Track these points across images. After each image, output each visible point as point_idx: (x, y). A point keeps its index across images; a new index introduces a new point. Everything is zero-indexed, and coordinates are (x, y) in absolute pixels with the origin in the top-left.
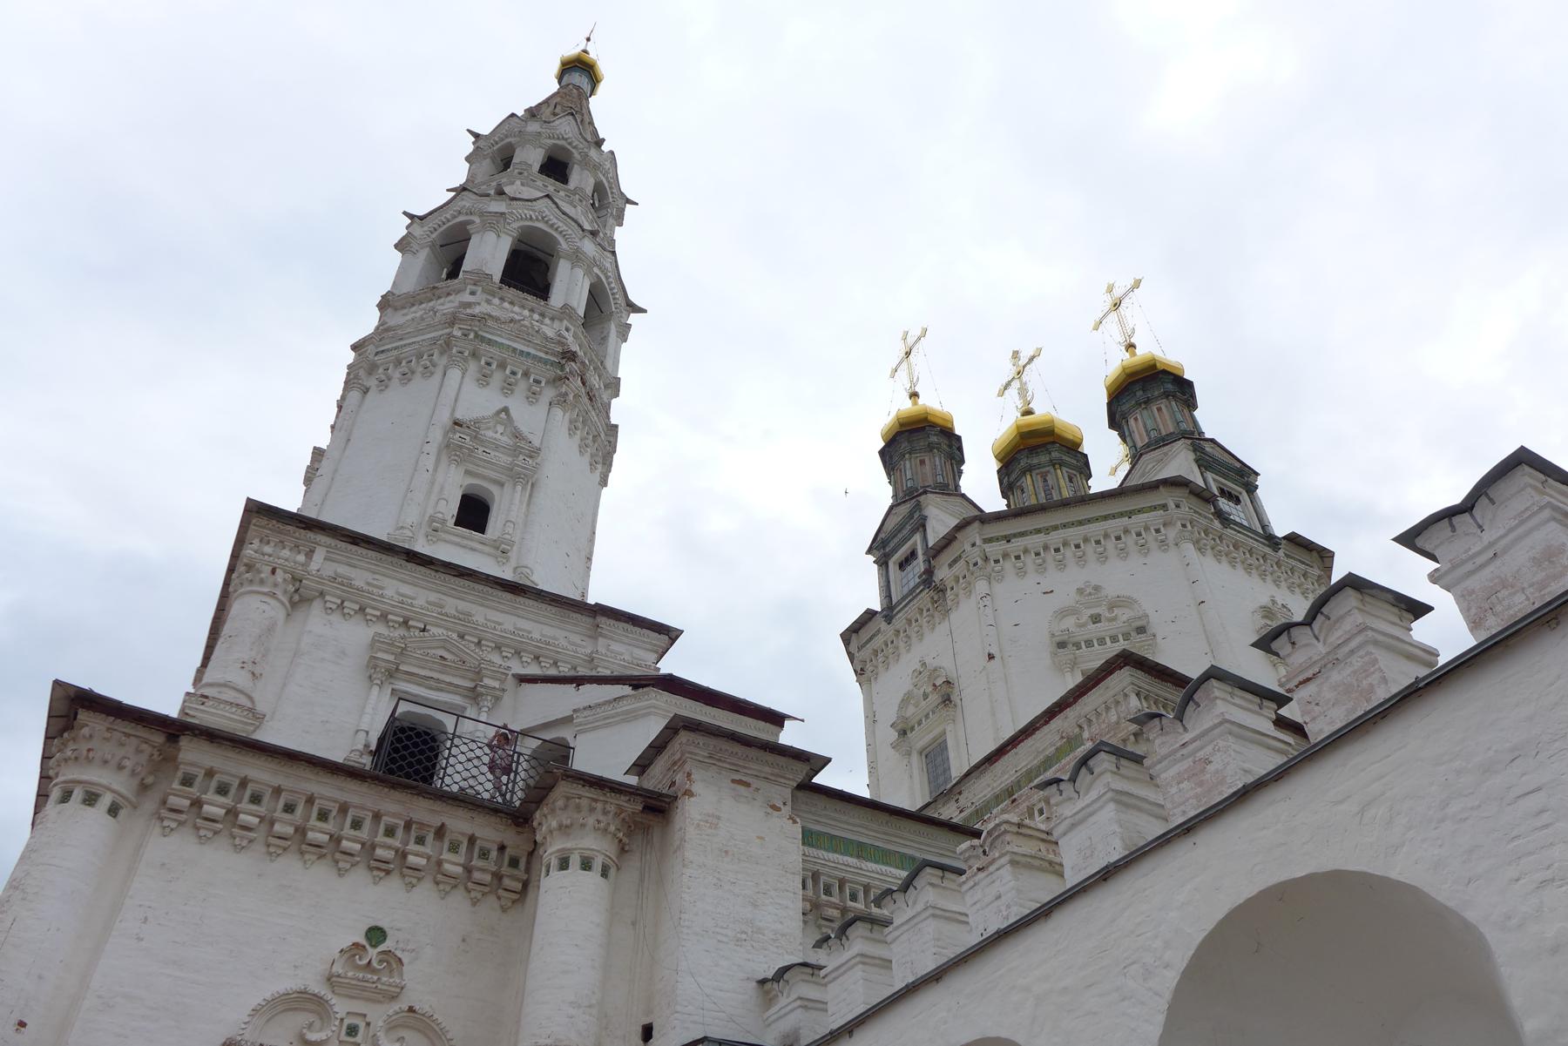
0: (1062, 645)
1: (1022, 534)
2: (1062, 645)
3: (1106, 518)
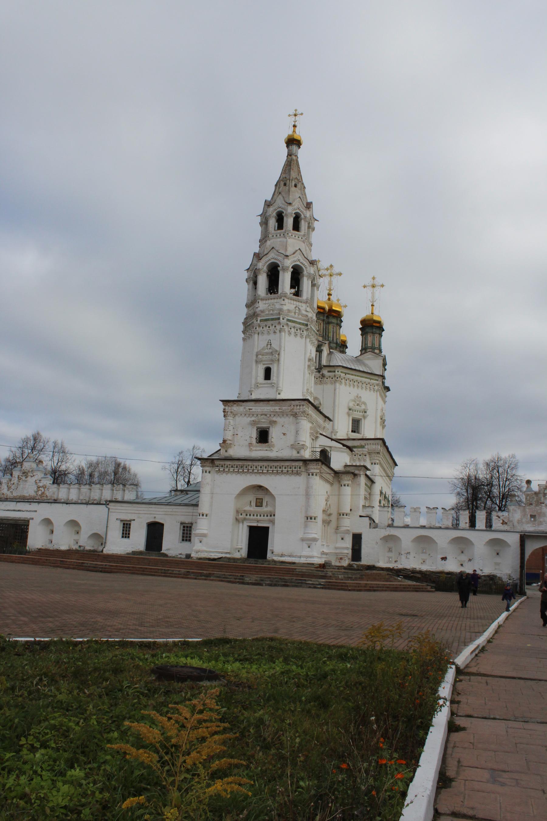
0: (350, 409)
1: (349, 374)
2: (350, 409)
3: (366, 378)
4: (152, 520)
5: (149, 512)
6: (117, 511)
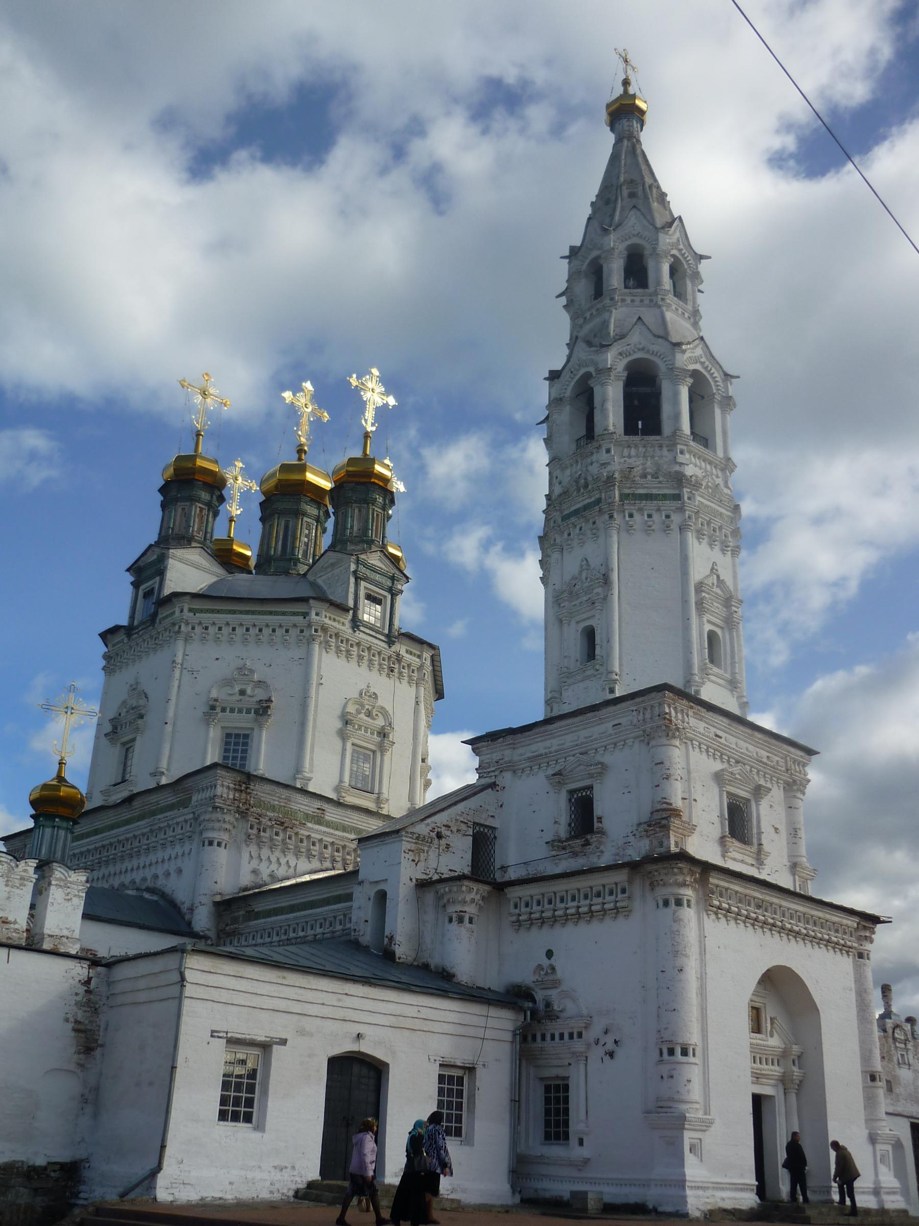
4: (349, 1046)
5: (340, 1014)
6: (215, 994)
